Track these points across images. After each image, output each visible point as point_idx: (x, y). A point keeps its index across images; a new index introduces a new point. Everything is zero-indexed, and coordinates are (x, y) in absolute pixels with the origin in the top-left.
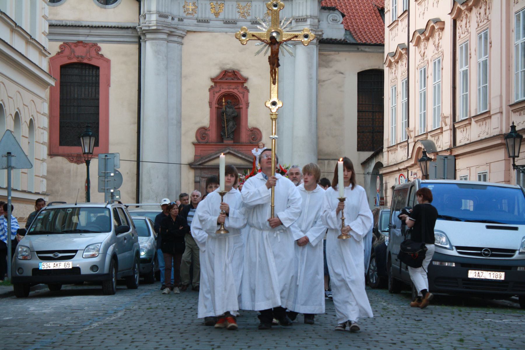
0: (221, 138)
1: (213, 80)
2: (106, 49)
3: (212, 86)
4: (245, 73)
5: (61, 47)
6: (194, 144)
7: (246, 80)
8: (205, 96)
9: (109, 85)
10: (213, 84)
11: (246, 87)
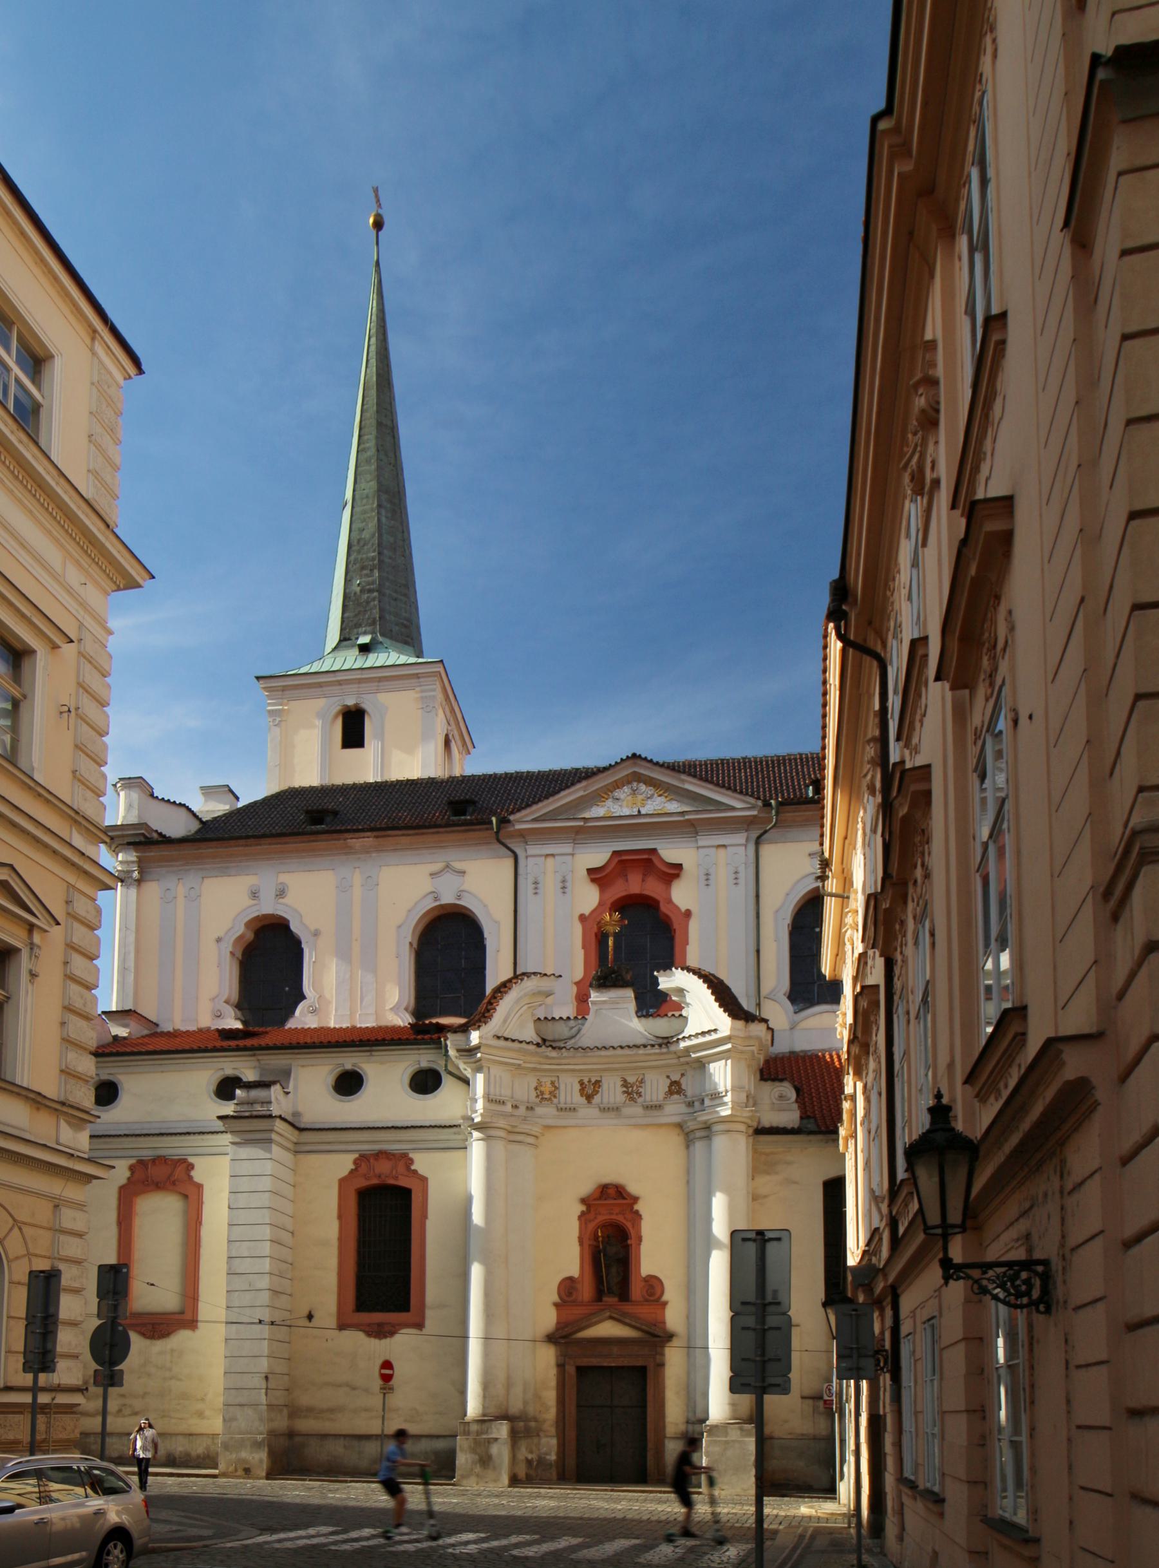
0: (599, 1294)
1: (583, 1201)
2: (422, 1163)
3: (583, 1214)
4: (633, 1188)
5: (355, 1162)
6: (556, 1305)
7: (636, 1199)
8: (571, 1229)
9: (424, 1216)
10: (584, 1208)
11: (637, 1212)
